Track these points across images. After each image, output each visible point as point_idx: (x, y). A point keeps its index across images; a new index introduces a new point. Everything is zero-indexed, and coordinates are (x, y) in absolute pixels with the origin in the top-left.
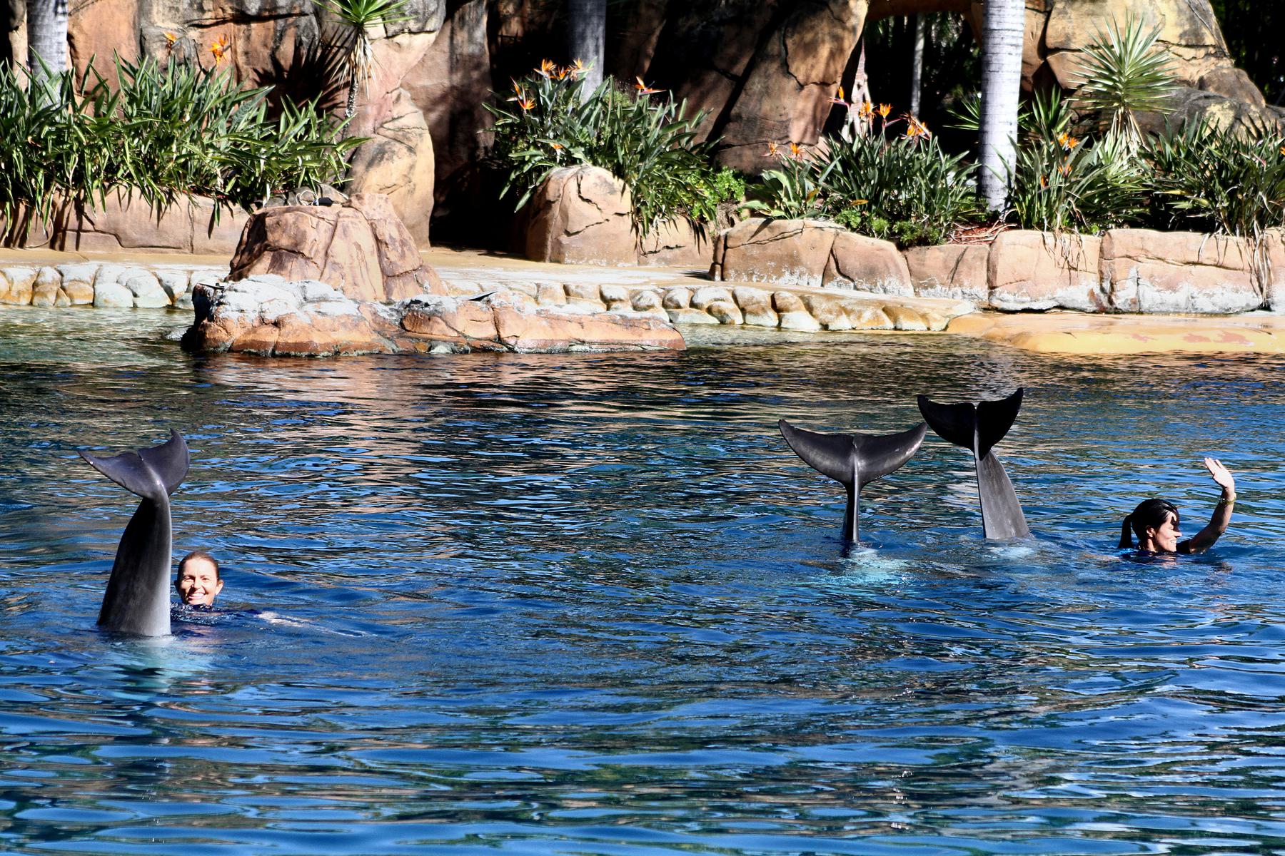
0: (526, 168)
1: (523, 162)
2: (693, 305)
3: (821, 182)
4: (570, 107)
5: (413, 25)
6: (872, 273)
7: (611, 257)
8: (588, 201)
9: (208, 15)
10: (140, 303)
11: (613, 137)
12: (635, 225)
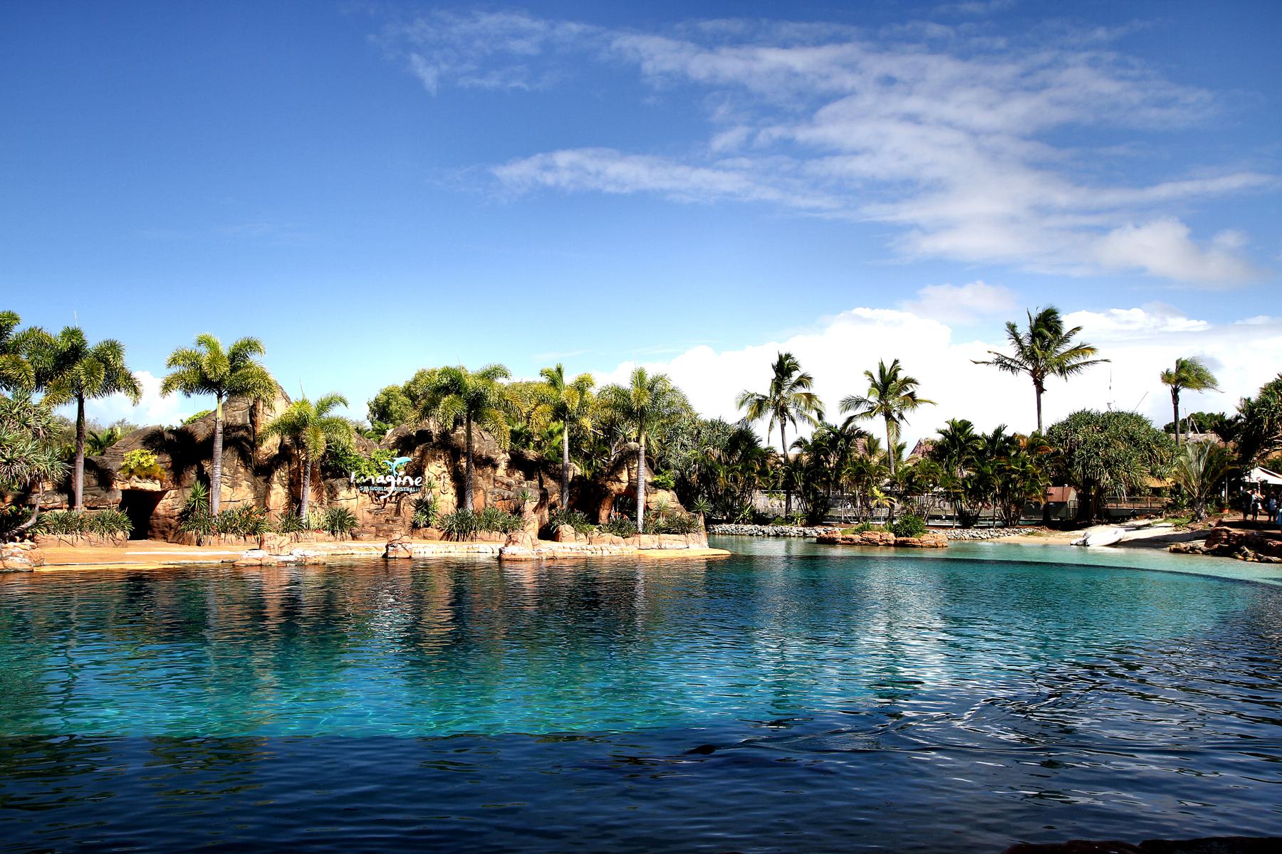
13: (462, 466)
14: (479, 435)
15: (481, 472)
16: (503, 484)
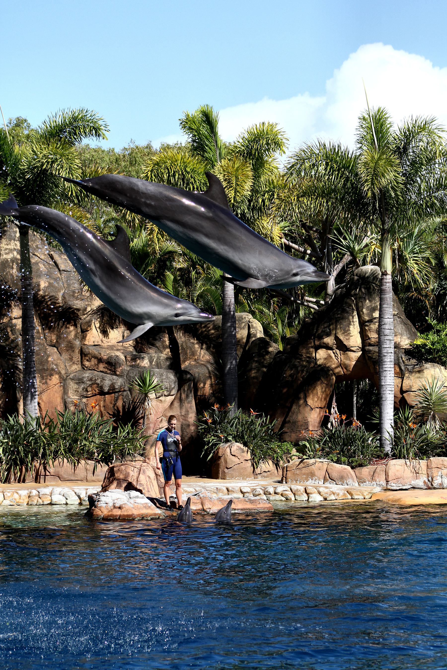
0: (210, 445)
1: (209, 442)
2: (275, 493)
3: (321, 444)
4: (226, 421)
5: (166, 393)
6: (342, 479)
7: (244, 477)
8: (234, 456)
9: (89, 393)
10: (68, 502)
11: (243, 431)
12: (253, 465)
13: (13, 327)
15: (54, 337)
16: (100, 360)
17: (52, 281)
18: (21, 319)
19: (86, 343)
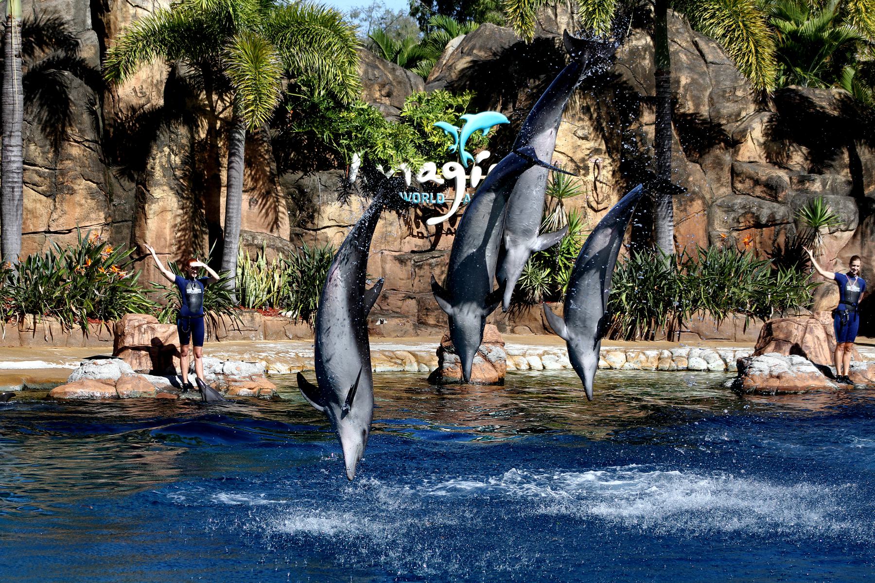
5: (843, 227)
9: (741, 225)
13: (643, 138)
14: (693, 49)
16: (757, 182)
17: (696, 77)
18: (654, 126)
19: (739, 158)
